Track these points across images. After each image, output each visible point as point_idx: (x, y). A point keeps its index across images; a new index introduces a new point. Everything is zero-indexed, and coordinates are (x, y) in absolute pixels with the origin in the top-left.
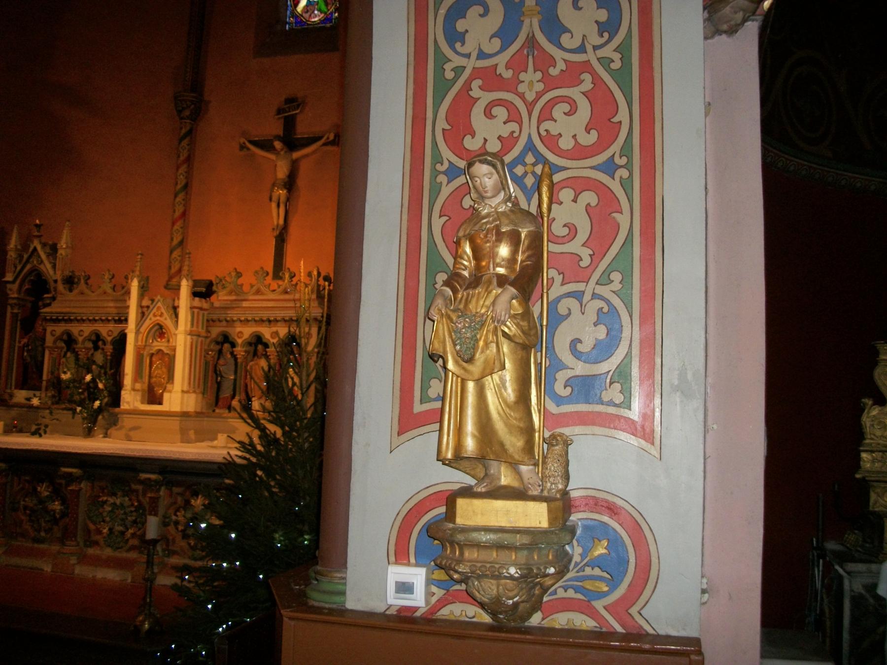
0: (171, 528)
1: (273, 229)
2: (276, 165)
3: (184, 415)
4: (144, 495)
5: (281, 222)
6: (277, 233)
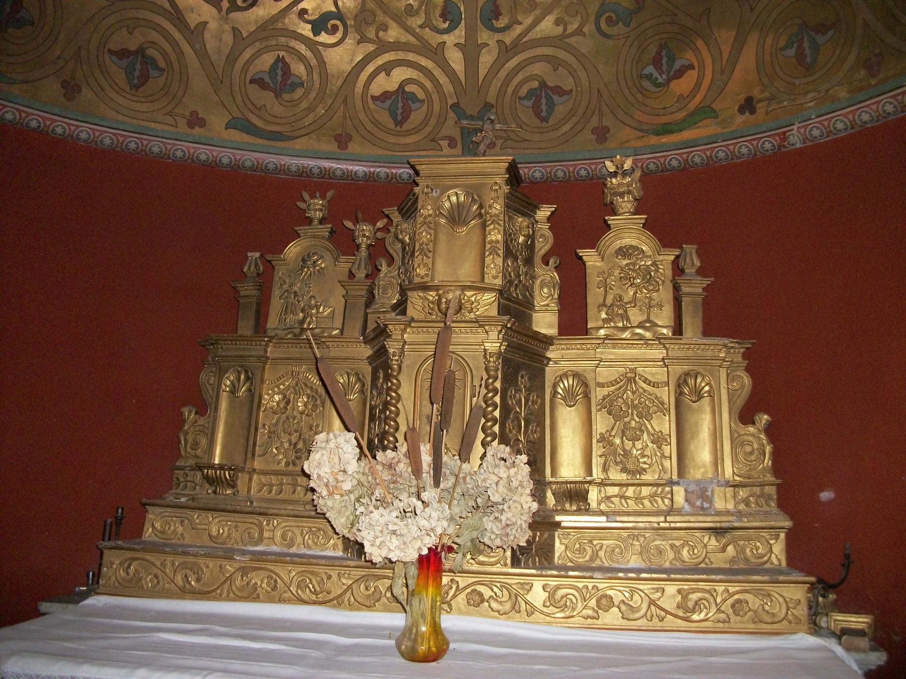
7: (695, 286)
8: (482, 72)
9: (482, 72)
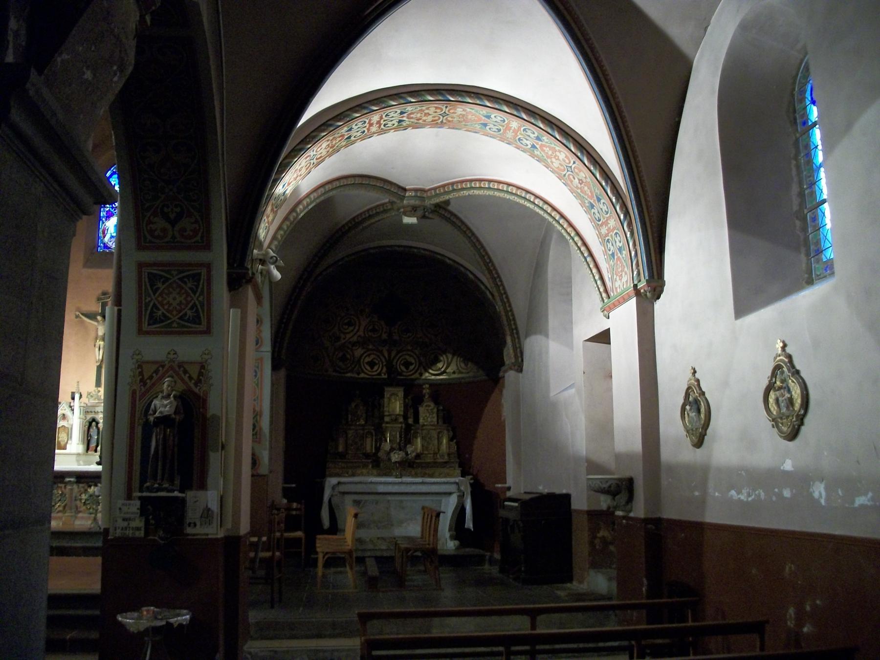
0: (78, 502)
1: (97, 362)
2: (98, 329)
3: (78, 454)
4: (65, 487)
5: (101, 358)
6: (98, 364)
7: (441, 414)
8: (392, 357)
9: (392, 357)
